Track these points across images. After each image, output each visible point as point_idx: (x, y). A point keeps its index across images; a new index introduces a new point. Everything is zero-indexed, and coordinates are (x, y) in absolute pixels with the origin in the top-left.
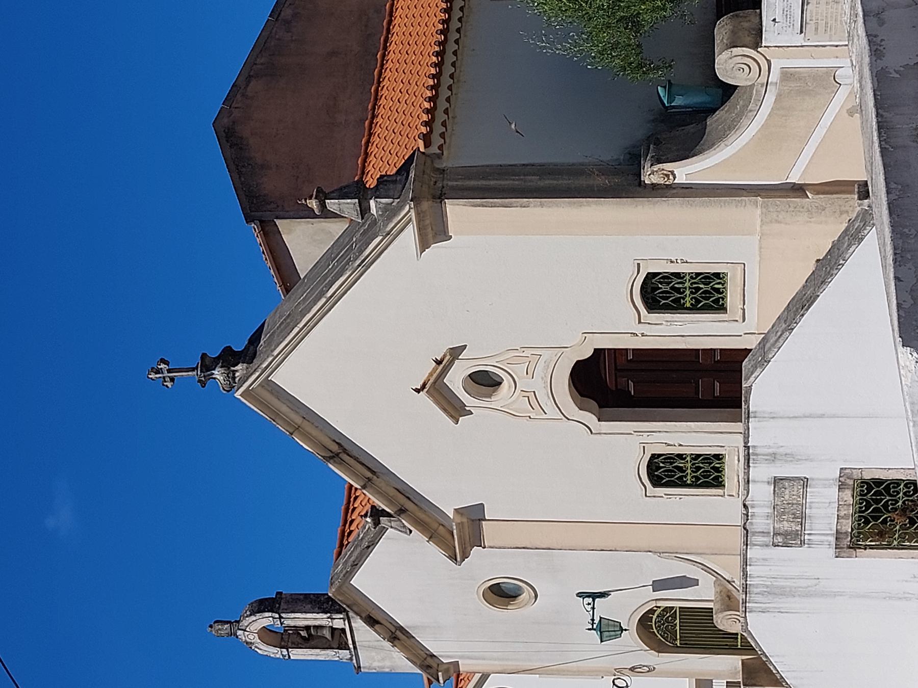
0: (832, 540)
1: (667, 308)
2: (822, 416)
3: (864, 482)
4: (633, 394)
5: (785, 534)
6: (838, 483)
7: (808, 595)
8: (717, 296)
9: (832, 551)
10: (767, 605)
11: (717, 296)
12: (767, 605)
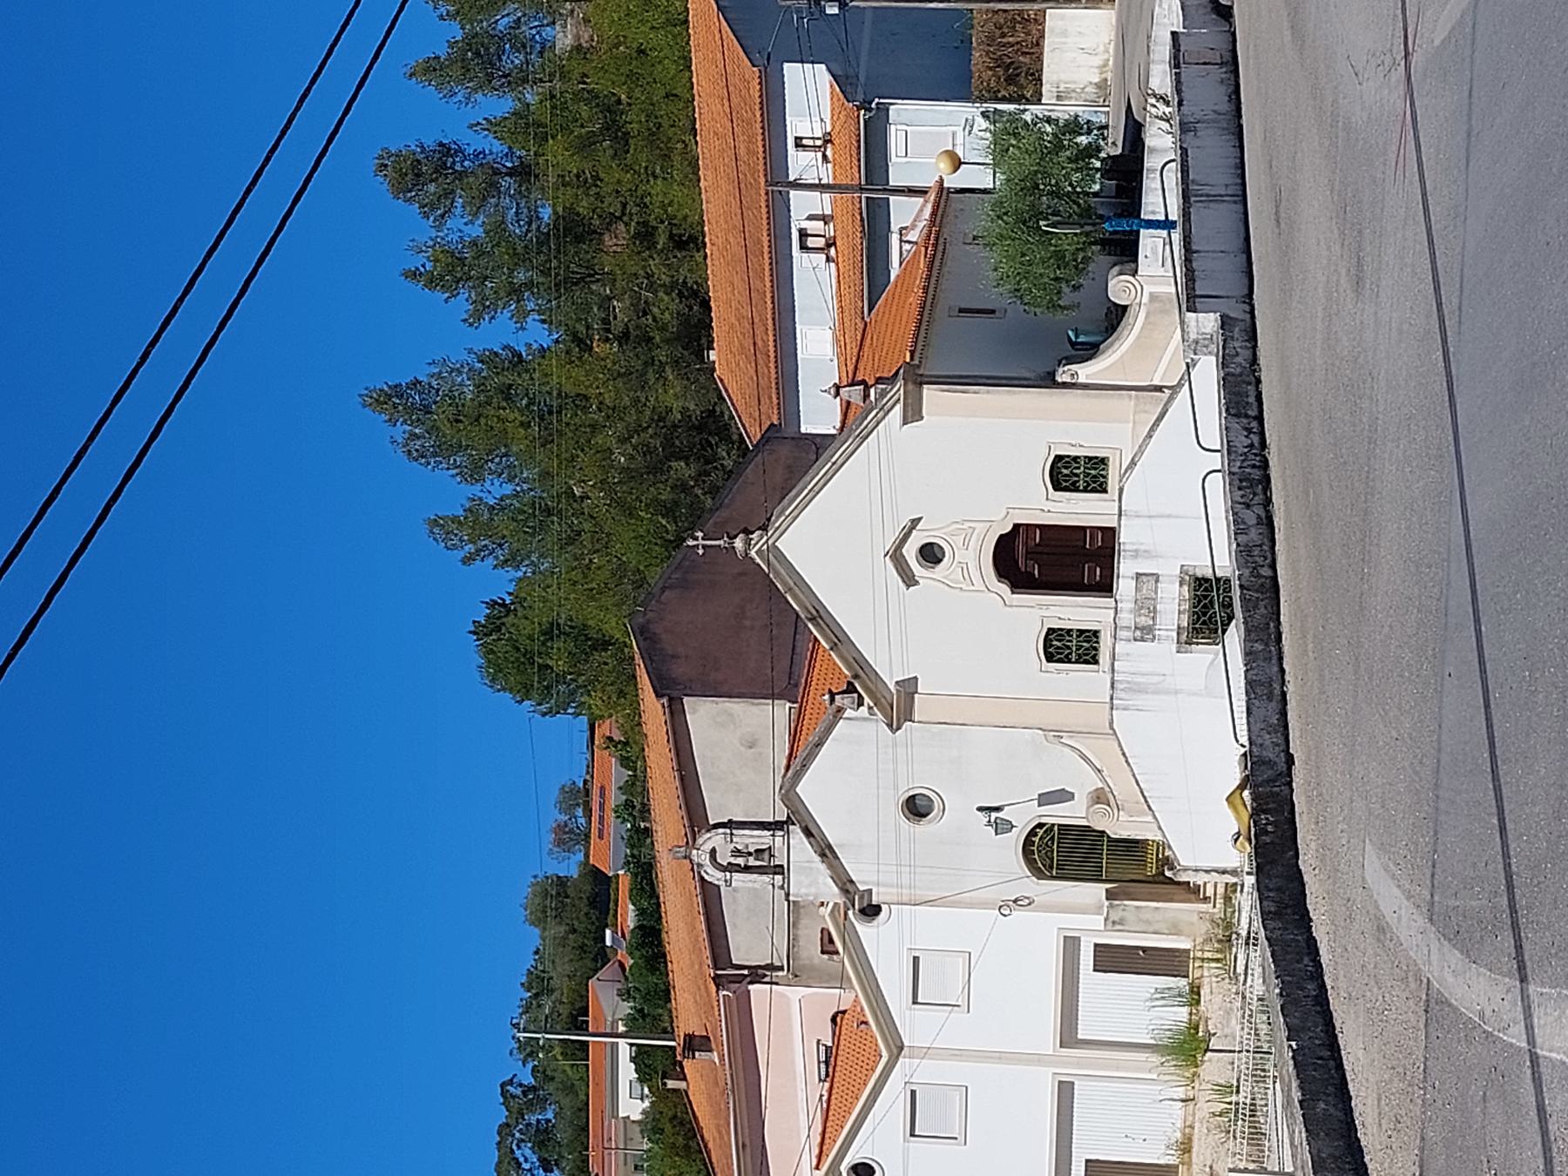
0: (1174, 634)
1: (1066, 489)
2: (1169, 516)
3: (1197, 579)
4: (1037, 576)
5: (1142, 629)
6: (1179, 579)
7: (1156, 692)
8: (1102, 480)
9: (1174, 647)
10: (1130, 702)
11: (1102, 480)
12: (1130, 702)
